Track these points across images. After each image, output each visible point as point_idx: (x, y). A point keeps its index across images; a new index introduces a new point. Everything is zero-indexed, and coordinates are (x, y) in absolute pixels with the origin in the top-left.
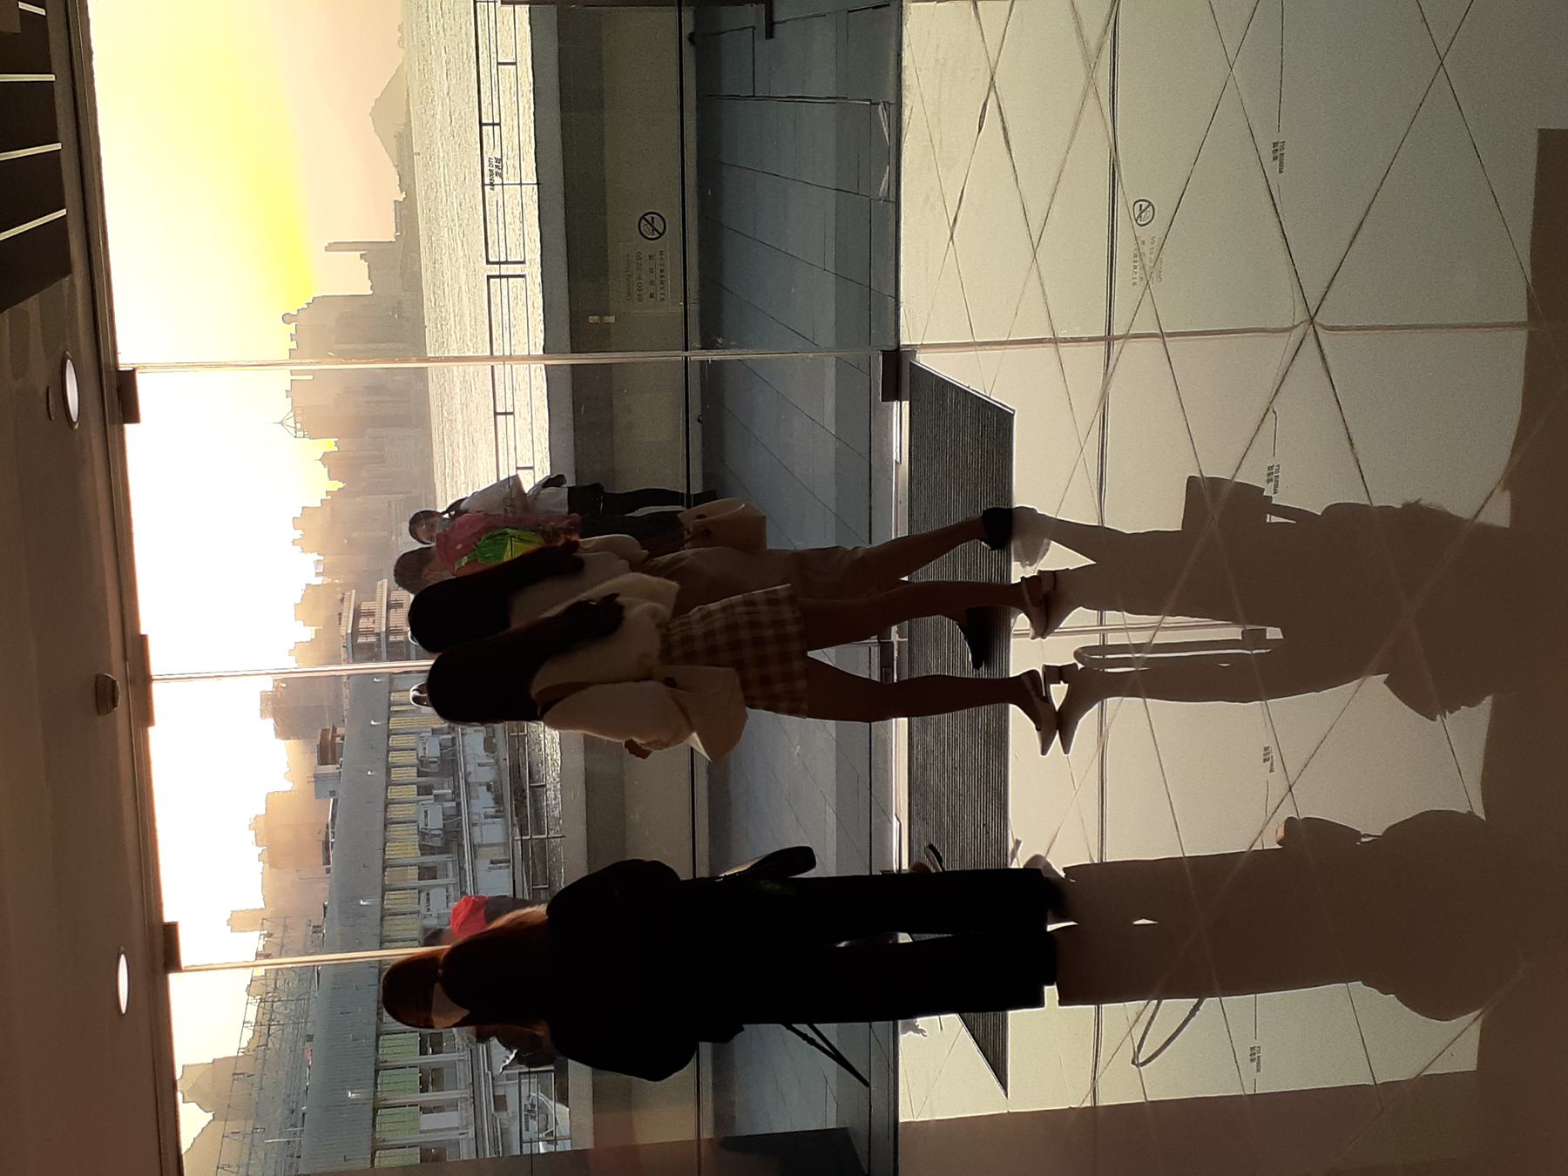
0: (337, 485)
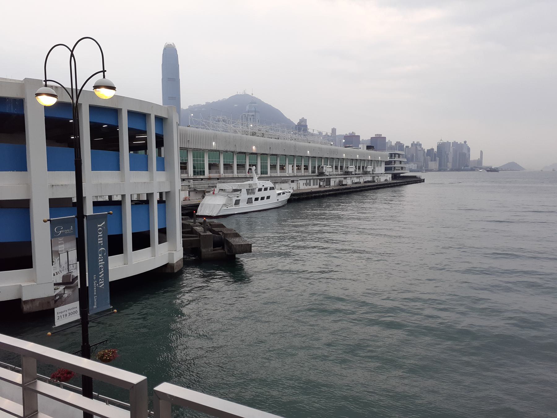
0: (426, 151)
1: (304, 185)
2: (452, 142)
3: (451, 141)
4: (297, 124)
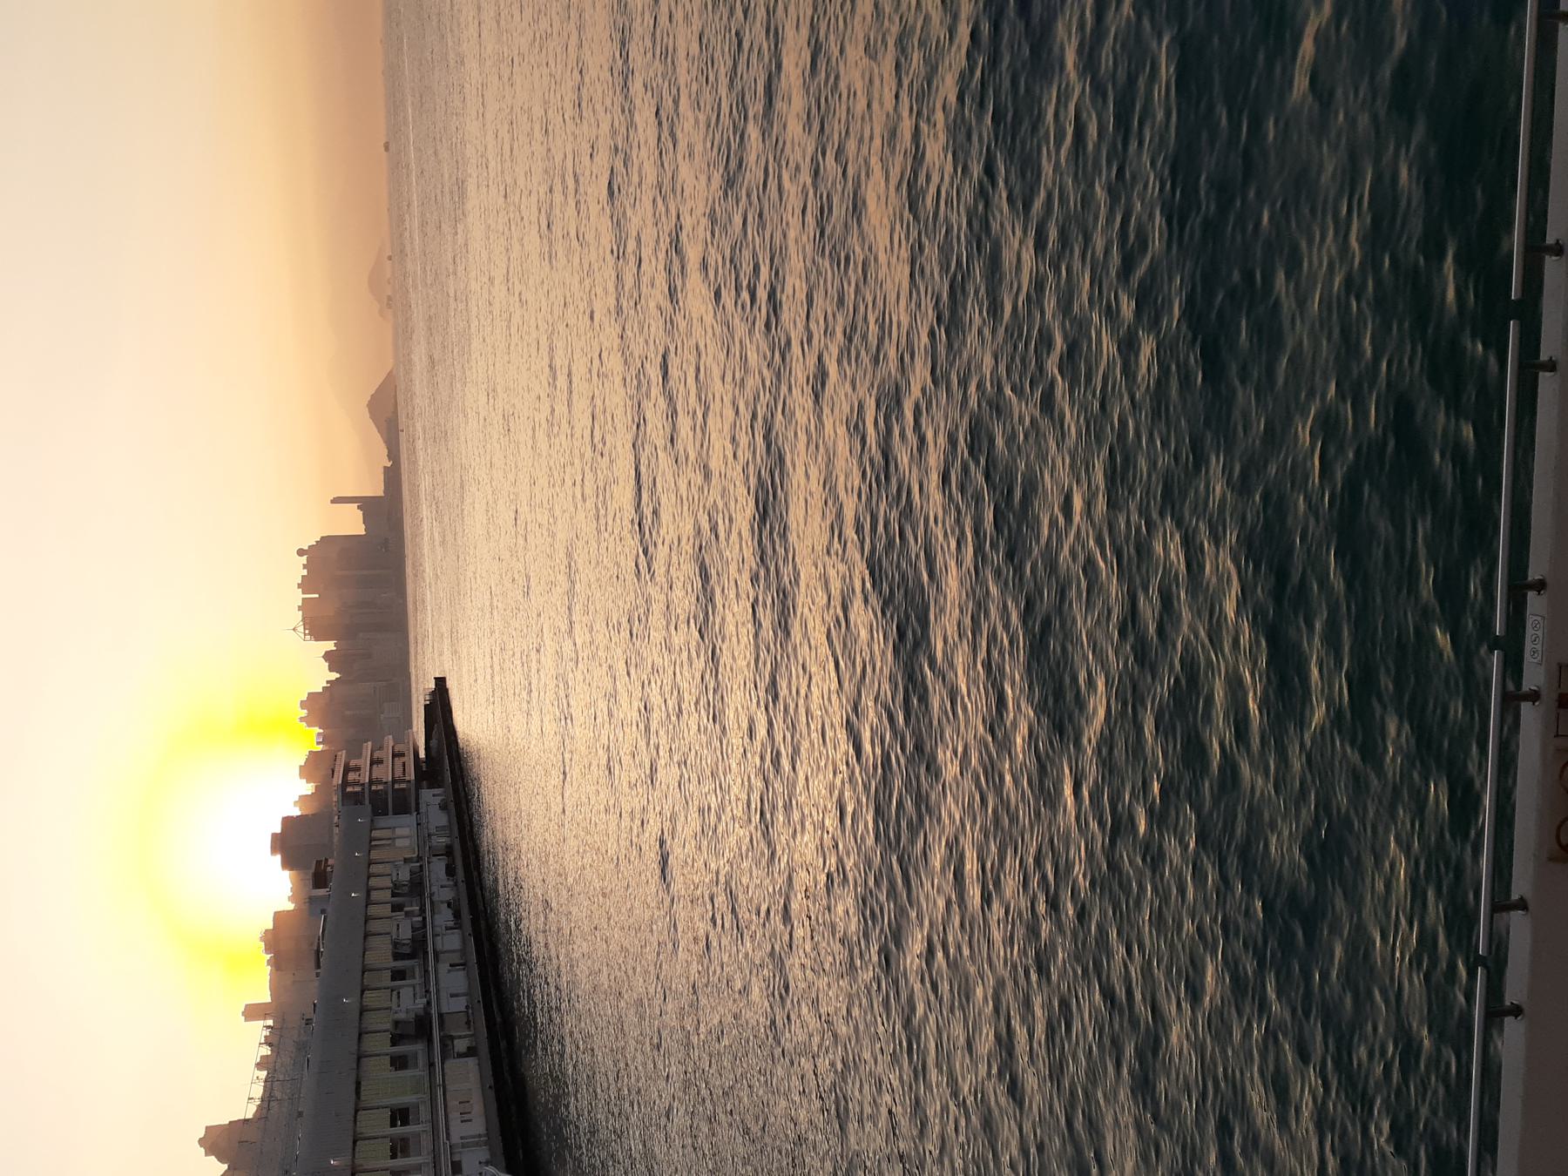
0: (335, 676)
1: (466, 1117)
2: (303, 593)
3: (298, 596)
4: (225, 1167)
